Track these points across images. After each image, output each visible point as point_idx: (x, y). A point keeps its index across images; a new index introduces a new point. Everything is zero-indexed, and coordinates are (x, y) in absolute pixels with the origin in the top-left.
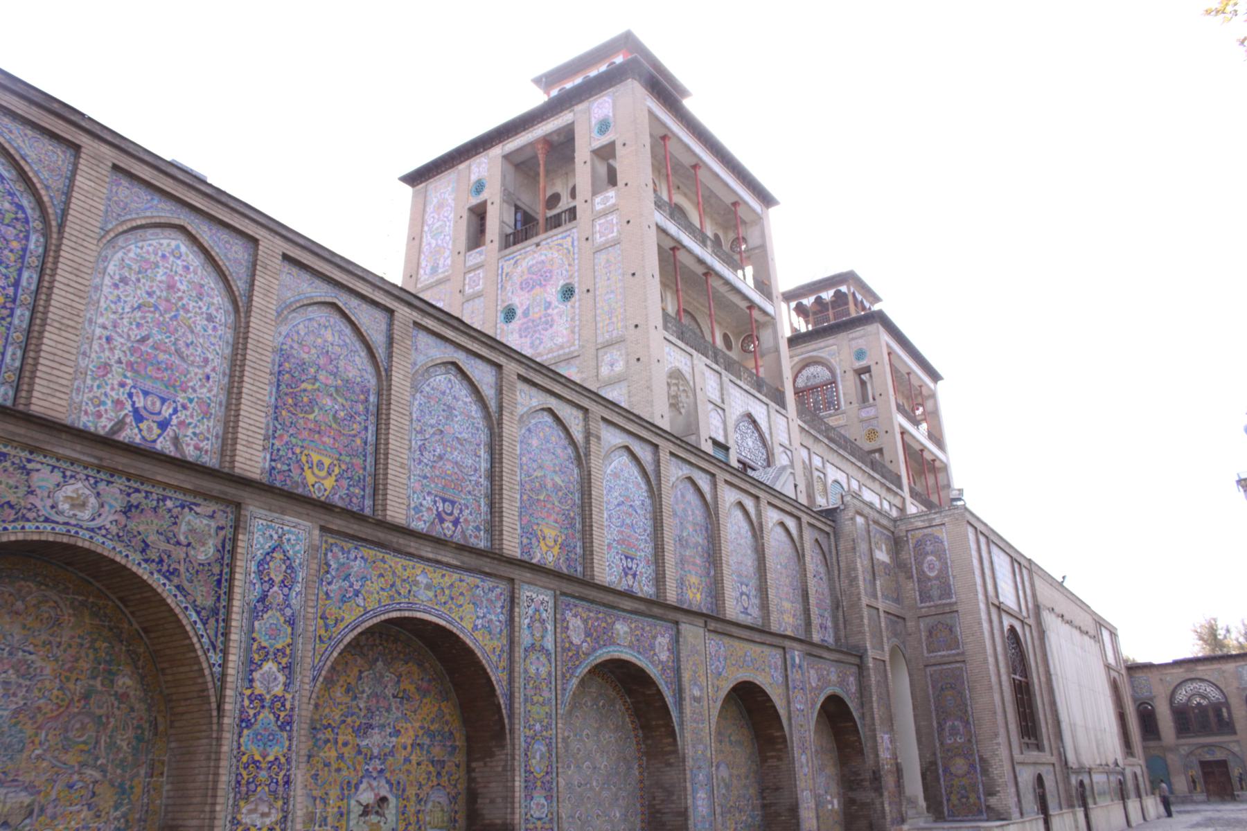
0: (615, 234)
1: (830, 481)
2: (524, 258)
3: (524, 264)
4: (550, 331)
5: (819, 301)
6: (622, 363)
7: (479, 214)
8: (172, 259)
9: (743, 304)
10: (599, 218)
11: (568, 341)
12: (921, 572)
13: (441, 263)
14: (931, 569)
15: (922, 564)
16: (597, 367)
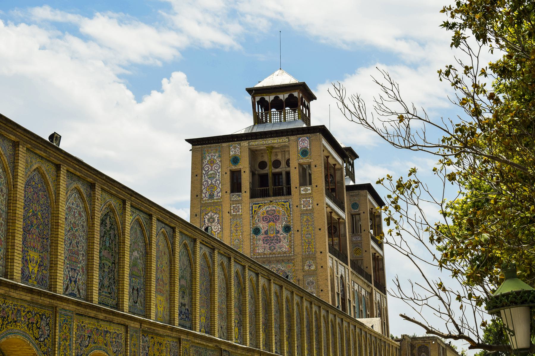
0: (311, 208)
2: (264, 206)
3: (264, 209)
6: (314, 266)
11: (288, 251)
13: (215, 193)
16: (303, 266)
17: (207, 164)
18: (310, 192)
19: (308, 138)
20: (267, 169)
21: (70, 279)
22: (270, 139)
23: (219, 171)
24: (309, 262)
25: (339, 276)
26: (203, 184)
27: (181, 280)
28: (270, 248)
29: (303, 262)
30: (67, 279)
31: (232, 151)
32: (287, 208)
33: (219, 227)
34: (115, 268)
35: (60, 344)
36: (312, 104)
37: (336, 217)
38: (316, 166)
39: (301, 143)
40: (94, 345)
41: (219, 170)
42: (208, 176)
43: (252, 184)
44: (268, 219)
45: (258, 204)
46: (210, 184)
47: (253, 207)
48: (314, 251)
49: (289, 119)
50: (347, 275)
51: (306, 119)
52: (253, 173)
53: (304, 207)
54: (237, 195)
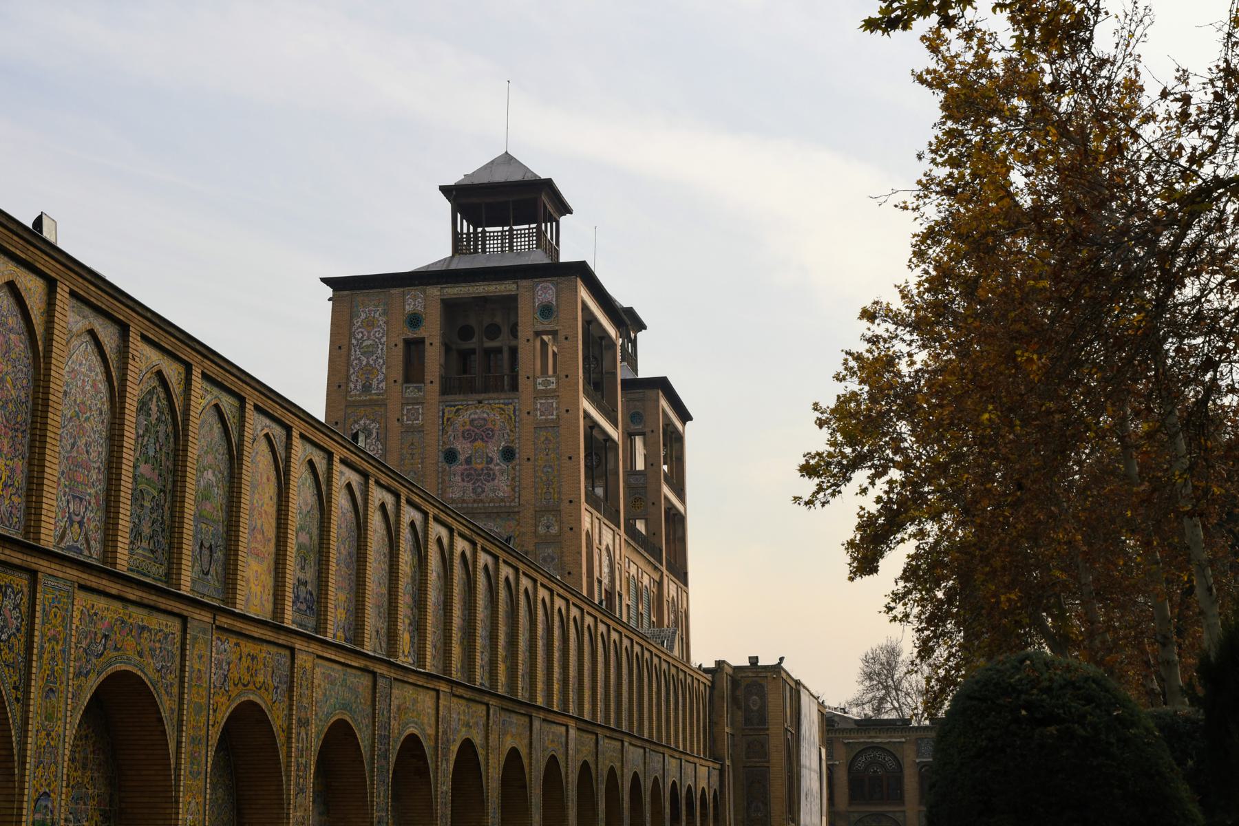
2: (466, 410)
3: (466, 416)
4: (491, 483)
6: (556, 528)
7: (414, 348)
10: (541, 398)
13: (375, 383)
16: (536, 526)
17: (360, 327)
18: (553, 386)
19: (553, 284)
20: (474, 340)
21: (70, 518)
22: (481, 283)
23: (382, 341)
24: (548, 520)
25: (603, 548)
26: (352, 365)
27: (300, 533)
28: (474, 491)
30: (63, 518)
31: (409, 305)
32: (509, 415)
33: (380, 447)
34: (165, 500)
35: (42, 647)
36: (564, 220)
37: (601, 437)
38: (566, 338)
39: (540, 293)
40: (116, 654)
41: (384, 339)
43: (446, 366)
45: (454, 406)
46: (366, 365)
47: (446, 411)
48: (559, 498)
49: (519, 248)
50: (617, 546)
51: (554, 251)
52: (447, 348)
53: (541, 415)
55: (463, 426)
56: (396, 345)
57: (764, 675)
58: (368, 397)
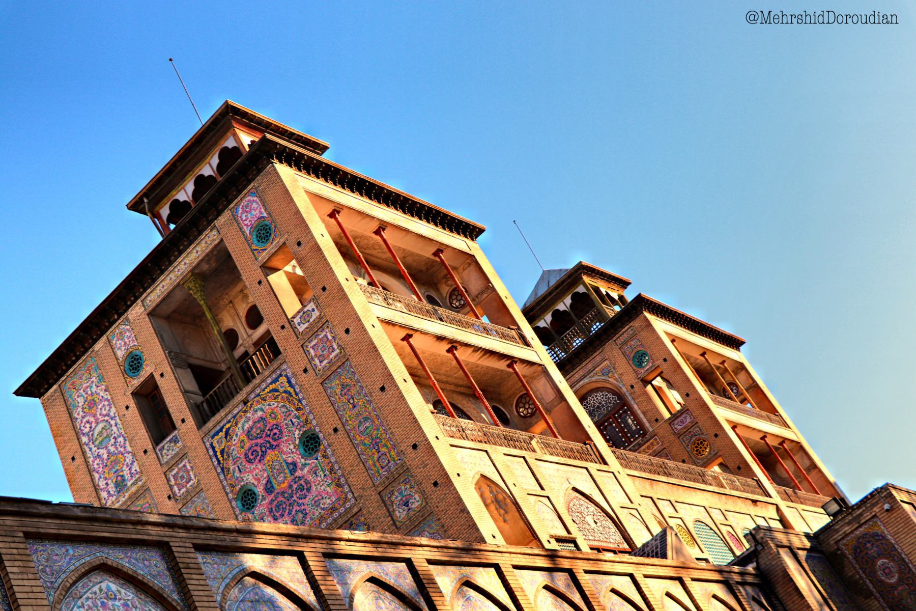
0: (337, 351)
1: (691, 526)
2: (236, 424)
3: (239, 432)
4: (310, 497)
5: (557, 314)
6: (417, 496)
8: (110, 603)
9: (502, 365)
11: (338, 499)
12: (879, 583)
13: (126, 472)
14: (889, 574)
15: (875, 572)
17: (83, 417)
18: (316, 314)
22: (180, 259)
23: (112, 414)
24: (400, 493)
29: (383, 501)
31: (119, 348)
32: (285, 392)
39: (244, 218)
41: (113, 410)
42: (97, 443)
44: (258, 449)
45: (221, 430)
48: (398, 454)
53: (321, 362)
54: (170, 442)
55: (242, 447)
56: (127, 407)
57: (868, 516)
58: (127, 495)
